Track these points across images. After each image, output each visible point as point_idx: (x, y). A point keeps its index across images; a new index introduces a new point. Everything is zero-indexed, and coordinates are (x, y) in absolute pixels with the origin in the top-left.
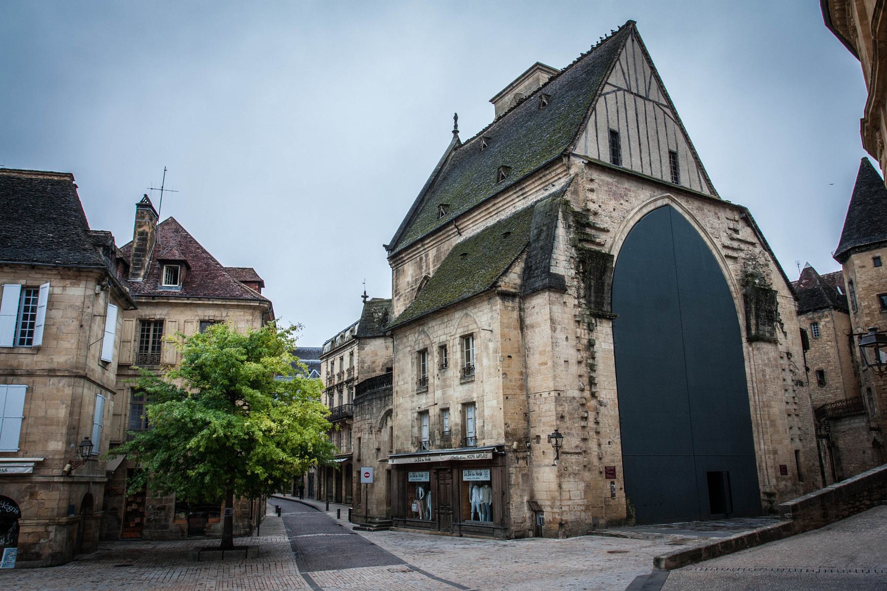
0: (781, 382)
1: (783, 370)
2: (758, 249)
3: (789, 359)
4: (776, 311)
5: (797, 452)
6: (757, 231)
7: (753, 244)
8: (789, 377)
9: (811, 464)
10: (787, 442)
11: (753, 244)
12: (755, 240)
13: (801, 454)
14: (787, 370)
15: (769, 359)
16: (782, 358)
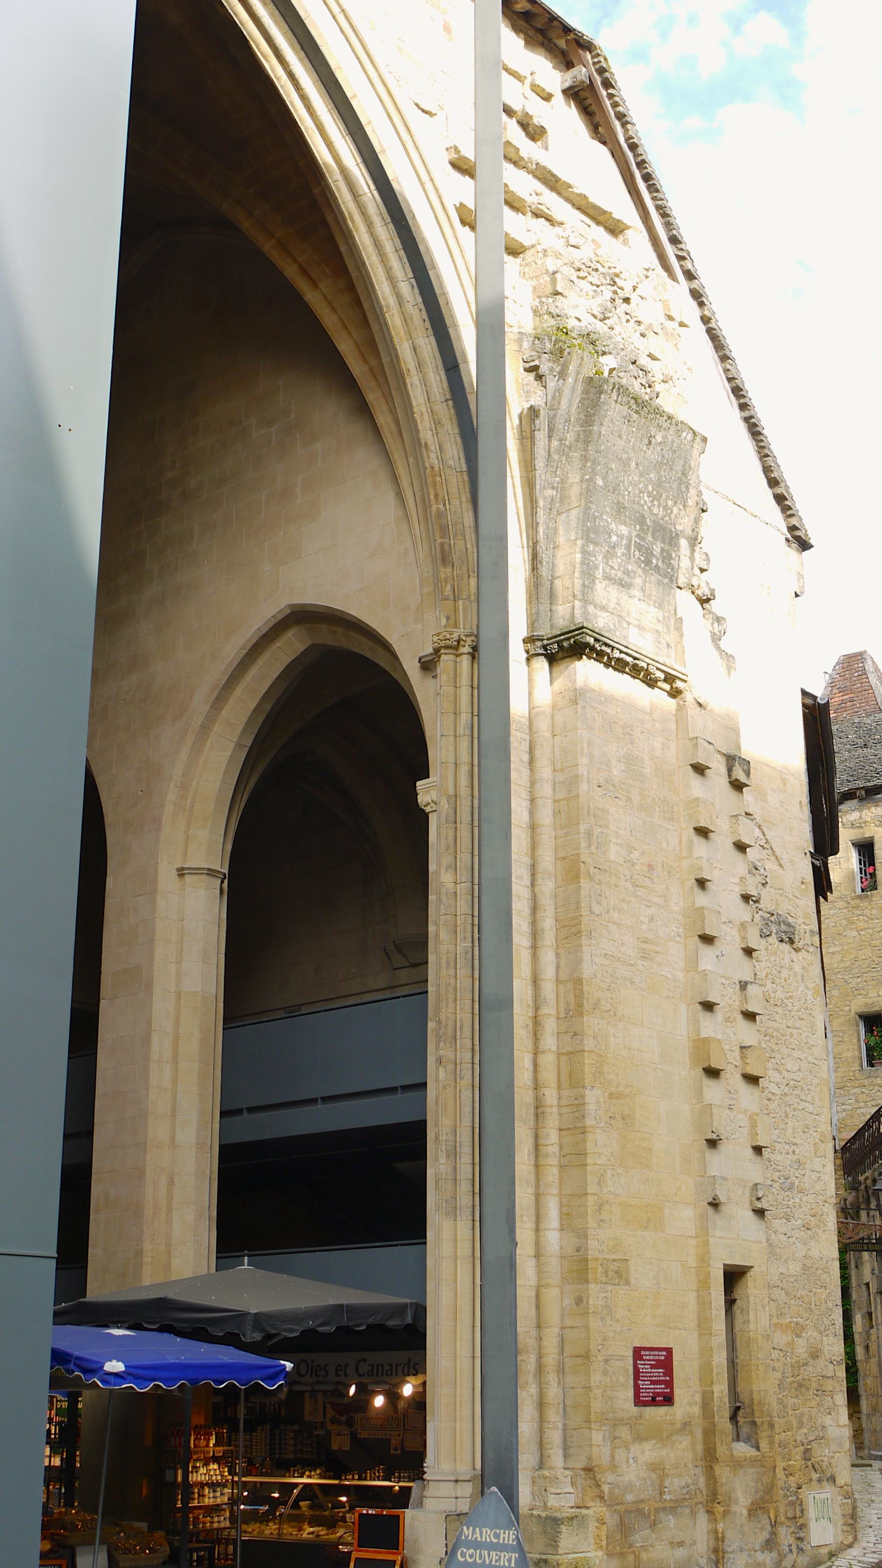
0: (679, 895)
1: (703, 832)
2: (634, 253)
3: (738, 786)
4: (694, 541)
5: (734, 1276)
6: (635, 172)
7: (615, 229)
8: (728, 875)
9: (802, 1348)
10: (684, 1217)
11: (615, 229)
12: (622, 207)
13: (751, 1290)
14: (723, 840)
15: (631, 761)
16: (699, 769)
